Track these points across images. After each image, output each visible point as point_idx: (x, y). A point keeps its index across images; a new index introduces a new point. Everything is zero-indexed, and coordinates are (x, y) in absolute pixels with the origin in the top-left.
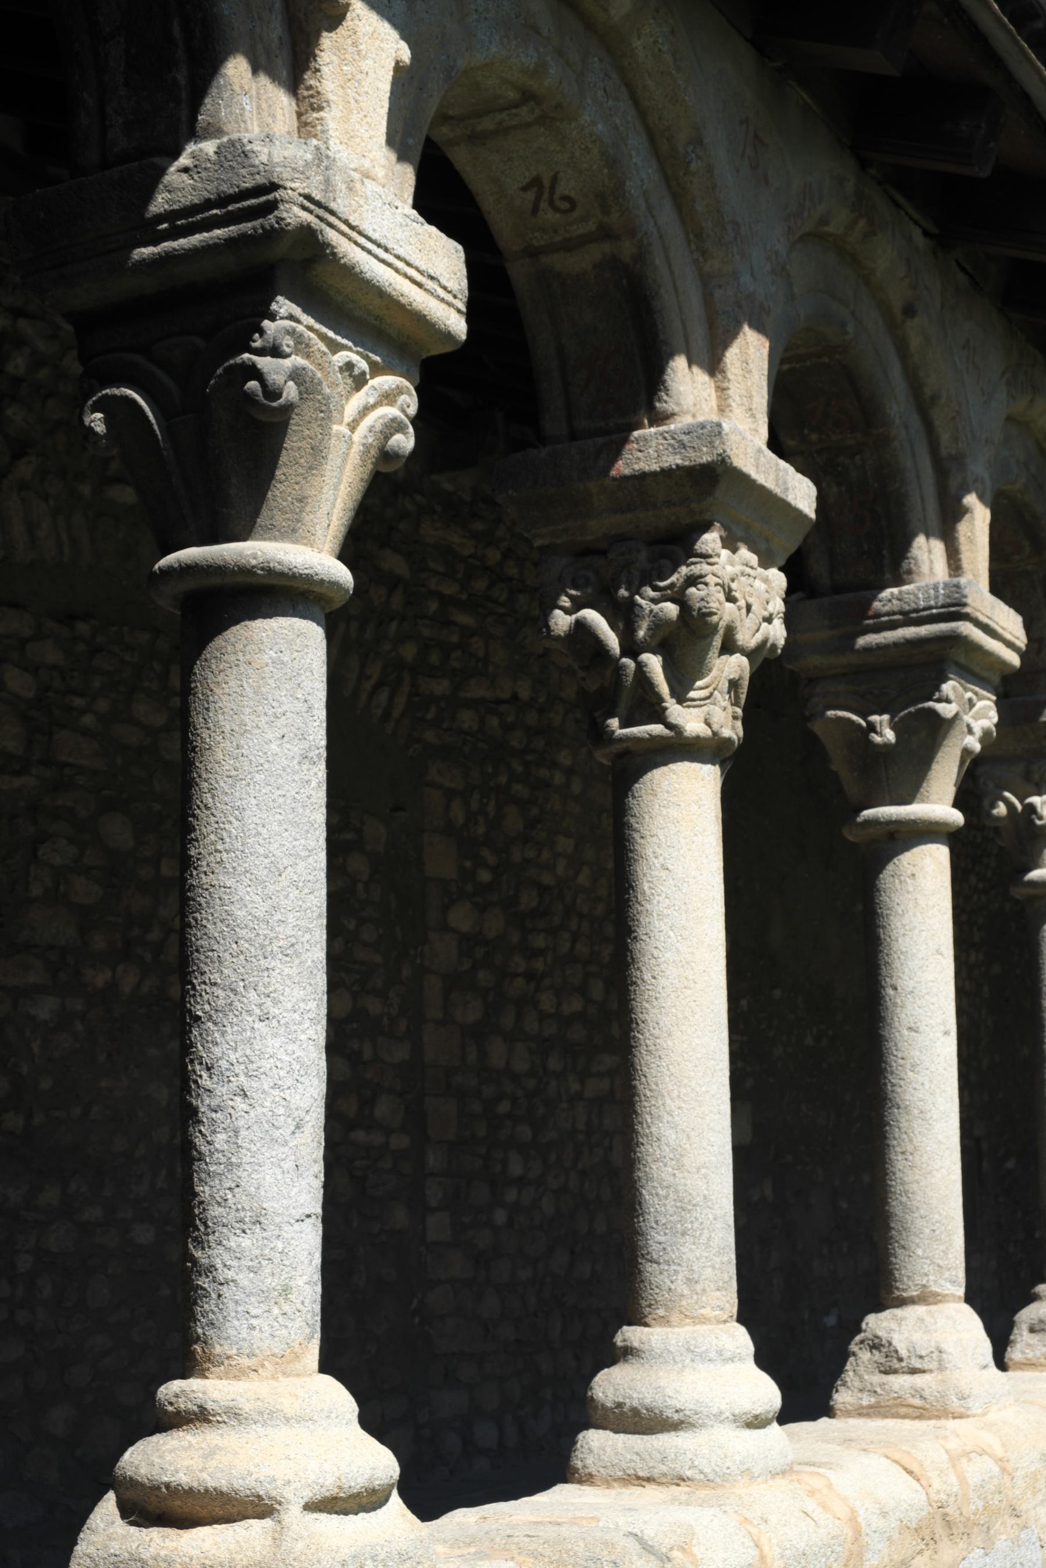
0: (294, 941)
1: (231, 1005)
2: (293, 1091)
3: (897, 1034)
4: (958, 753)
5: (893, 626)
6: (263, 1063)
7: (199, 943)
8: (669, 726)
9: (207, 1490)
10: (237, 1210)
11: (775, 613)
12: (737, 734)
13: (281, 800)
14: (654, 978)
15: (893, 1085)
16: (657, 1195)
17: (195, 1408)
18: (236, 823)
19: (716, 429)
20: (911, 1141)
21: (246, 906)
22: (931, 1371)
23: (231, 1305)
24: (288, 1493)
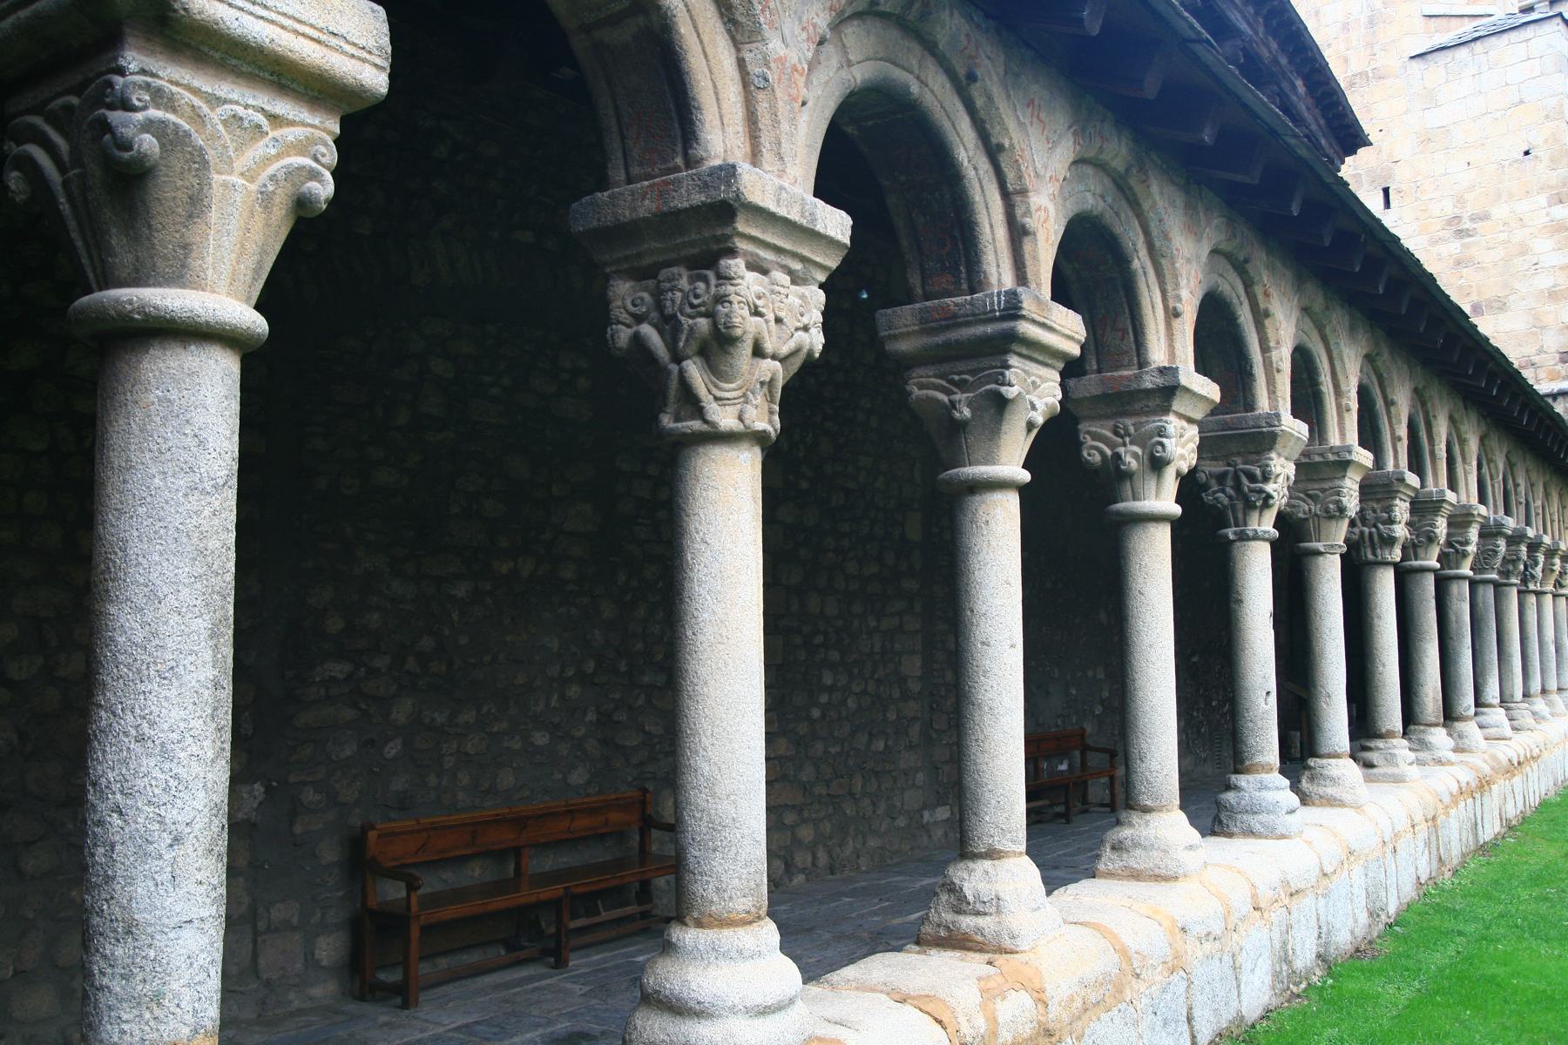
0: (175, 664)
1: (111, 725)
2: (169, 806)
4: (1024, 424)
5: (968, 324)
6: (138, 782)
10: (112, 921)
12: (773, 426)
13: (162, 531)
14: (694, 634)
15: (970, 687)
16: (694, 816)
18: (120, 554)
19: (731, 170)
20: (982, 731)
21: (126, 633)
22: (991, 914)
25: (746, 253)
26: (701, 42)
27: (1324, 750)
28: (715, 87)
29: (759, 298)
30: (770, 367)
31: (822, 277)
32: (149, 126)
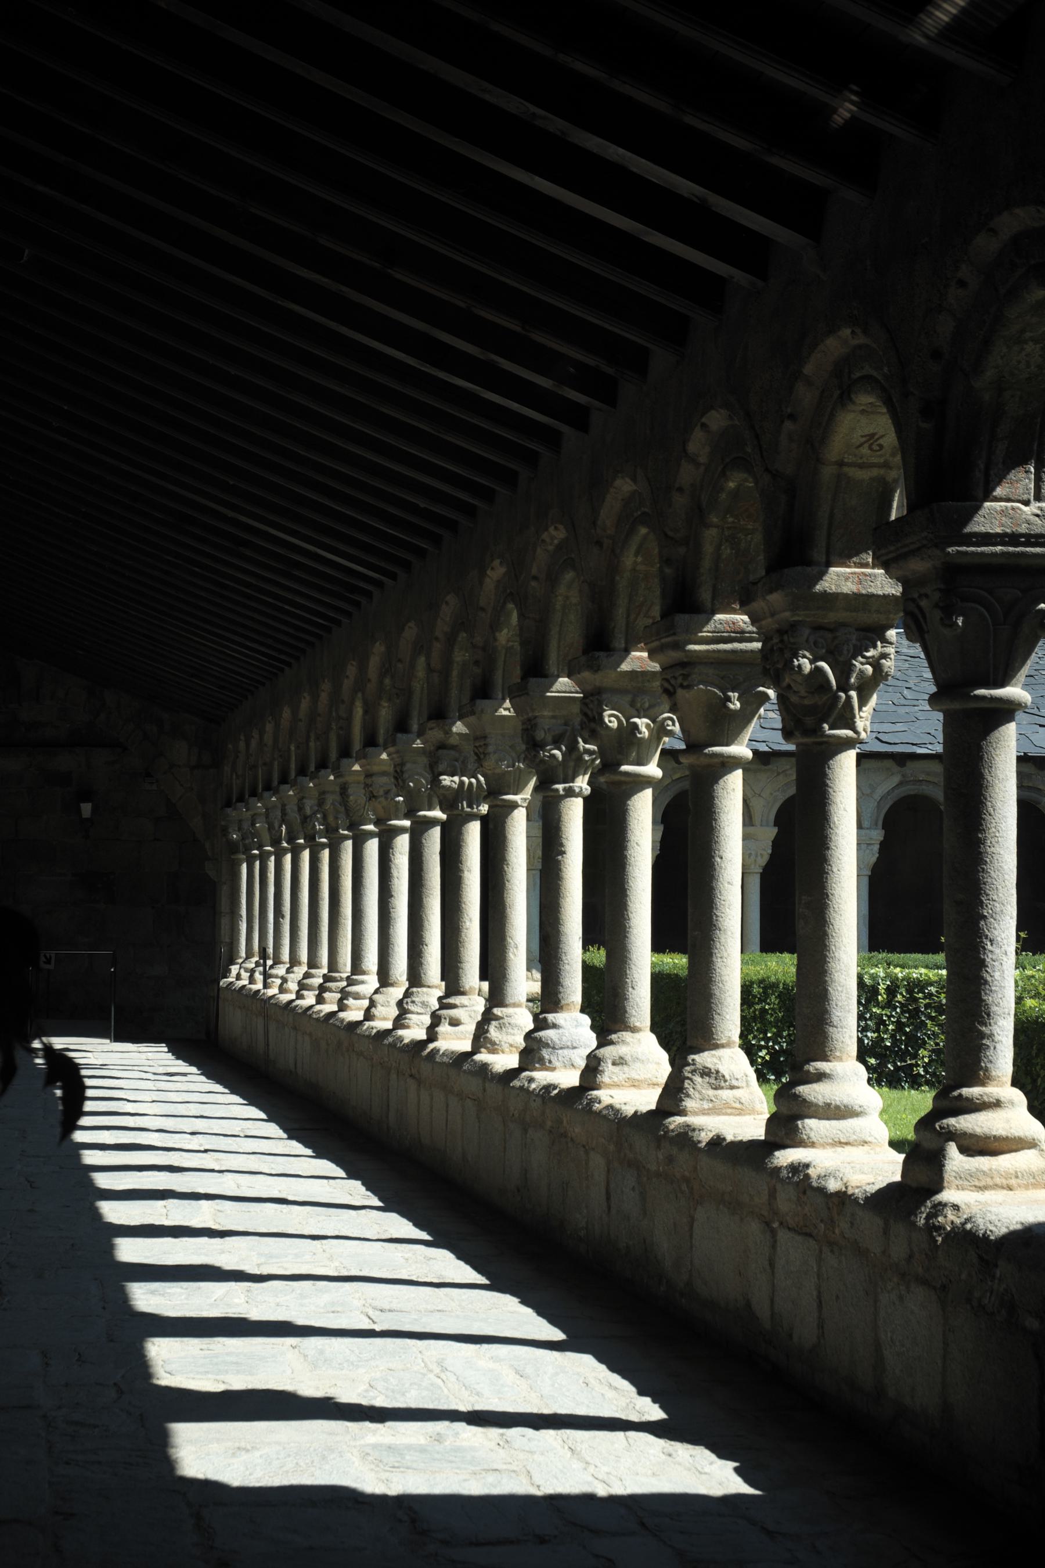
3: (721, 885)
7: (985, 880)
9: (1015, 1137)
14: (839, 870)
15: (717, 916)
16: (837, 990)
17: (995, 1101)
20: (726, 951)
22: (743, 1087)
23: (999, 1052)
27: (509, 1000)
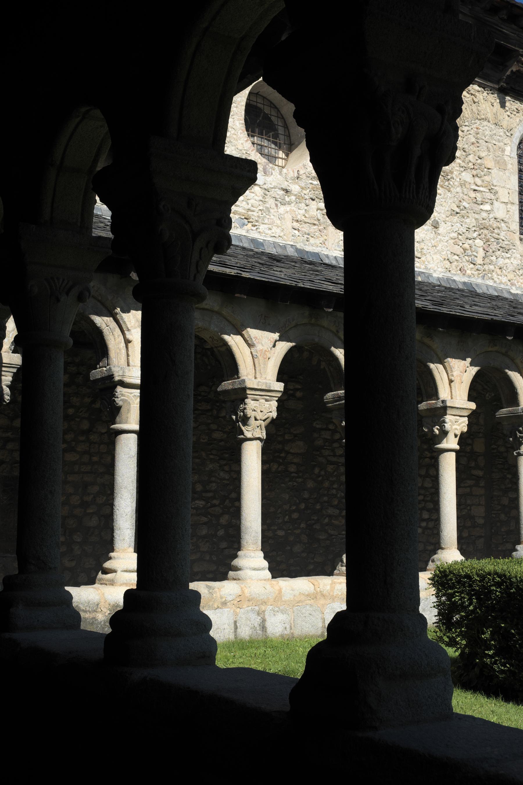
8: (244, 436)
11: (273, 410)
24: (118, 569)
25: (251, 398)
26: (240, 350)
28: (244, 359)
29: (255, 407)
30: (258, 423)
31: (277, 399)
32: (121, 400)
